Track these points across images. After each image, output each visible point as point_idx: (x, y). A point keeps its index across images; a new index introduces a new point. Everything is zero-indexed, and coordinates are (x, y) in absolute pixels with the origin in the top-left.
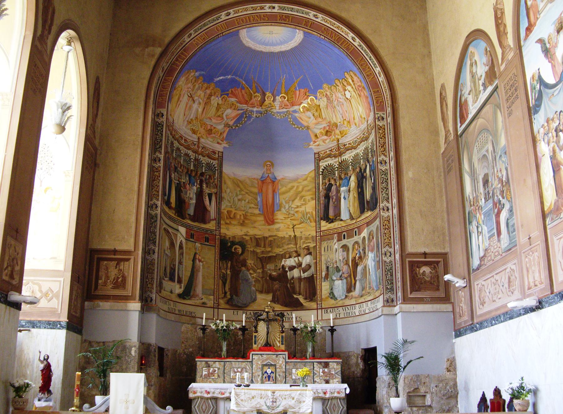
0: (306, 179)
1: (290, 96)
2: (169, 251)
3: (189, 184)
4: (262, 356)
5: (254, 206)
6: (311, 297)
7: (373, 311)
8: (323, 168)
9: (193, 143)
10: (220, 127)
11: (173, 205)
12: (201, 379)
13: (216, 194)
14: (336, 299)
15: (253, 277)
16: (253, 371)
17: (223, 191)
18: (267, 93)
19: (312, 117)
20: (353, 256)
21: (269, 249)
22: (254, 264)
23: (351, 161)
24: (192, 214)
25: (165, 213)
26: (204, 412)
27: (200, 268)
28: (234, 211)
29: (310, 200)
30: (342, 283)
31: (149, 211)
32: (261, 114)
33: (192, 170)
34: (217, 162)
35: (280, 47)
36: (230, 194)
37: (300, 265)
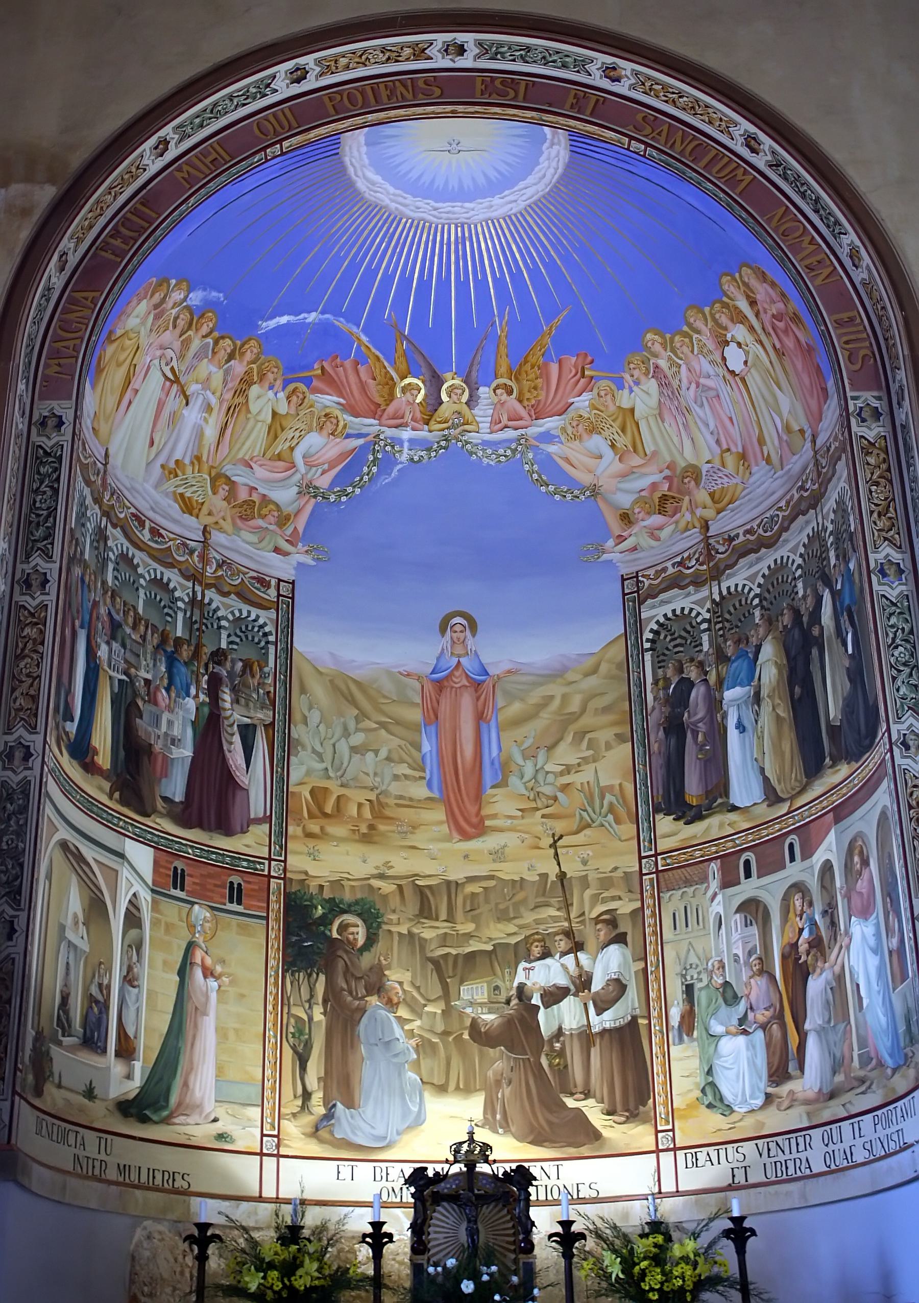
0: (594, 671)
1: (526, 384)
2: (82, 929)
3: (168, 690)
5: (409, 772)
6: (632, 1106)
7: (887, 1156)
8: (655, 627)
9: (185, 545)
10: (285, 496)
11: (104, 760)
14: (728, 1109)
15: (411, 1034)
17: (297, 716)
18: (448, 375)
19: (608, 453)
20: (786, 940)
21: (470, 927)
22: (412, 984)
23: (758, 591)
24: (179, 797)
25: (69, 789)
27: (207, 997)
28: (337, 791)
29: (613, 743)
30: (751, 1046)
32: (429, 450)
33: (178, 642)
34: (272, 614)
35: (486, 202)
36: (322, 728)
37: (583, 982)
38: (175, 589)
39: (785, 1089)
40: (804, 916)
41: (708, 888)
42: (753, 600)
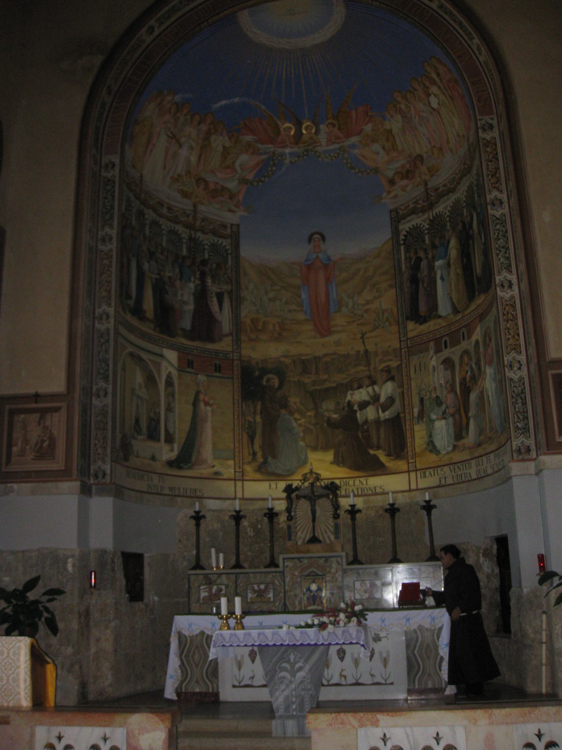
3: (180, 280)
4: (300, 562)
7: (499, 471)
8: (405, 233)
10: (232, 185)
12: (198, 604)
13: (230, 293)
14: (438, 452)
15: (300, 425)
16: (286, 588)
19: (382, 152)
21: (326, 377)
23: (448, 213)
26: (197, 665)
30: (447, 424)
31: (97, 325)
32: (299, 157)
33: (184, 258)
34: (229, 241)
37: (376, 398)
38: (181, 234)
39: (461, 443)
40: (469, 366)
41: (429, 354)
42: (446, 219)
